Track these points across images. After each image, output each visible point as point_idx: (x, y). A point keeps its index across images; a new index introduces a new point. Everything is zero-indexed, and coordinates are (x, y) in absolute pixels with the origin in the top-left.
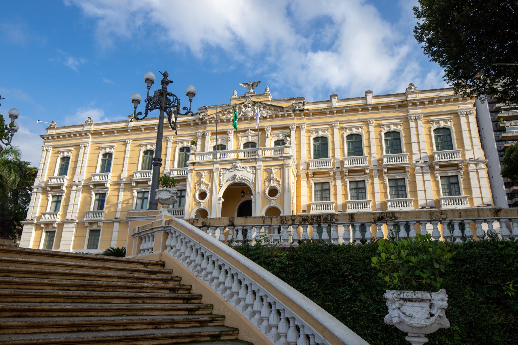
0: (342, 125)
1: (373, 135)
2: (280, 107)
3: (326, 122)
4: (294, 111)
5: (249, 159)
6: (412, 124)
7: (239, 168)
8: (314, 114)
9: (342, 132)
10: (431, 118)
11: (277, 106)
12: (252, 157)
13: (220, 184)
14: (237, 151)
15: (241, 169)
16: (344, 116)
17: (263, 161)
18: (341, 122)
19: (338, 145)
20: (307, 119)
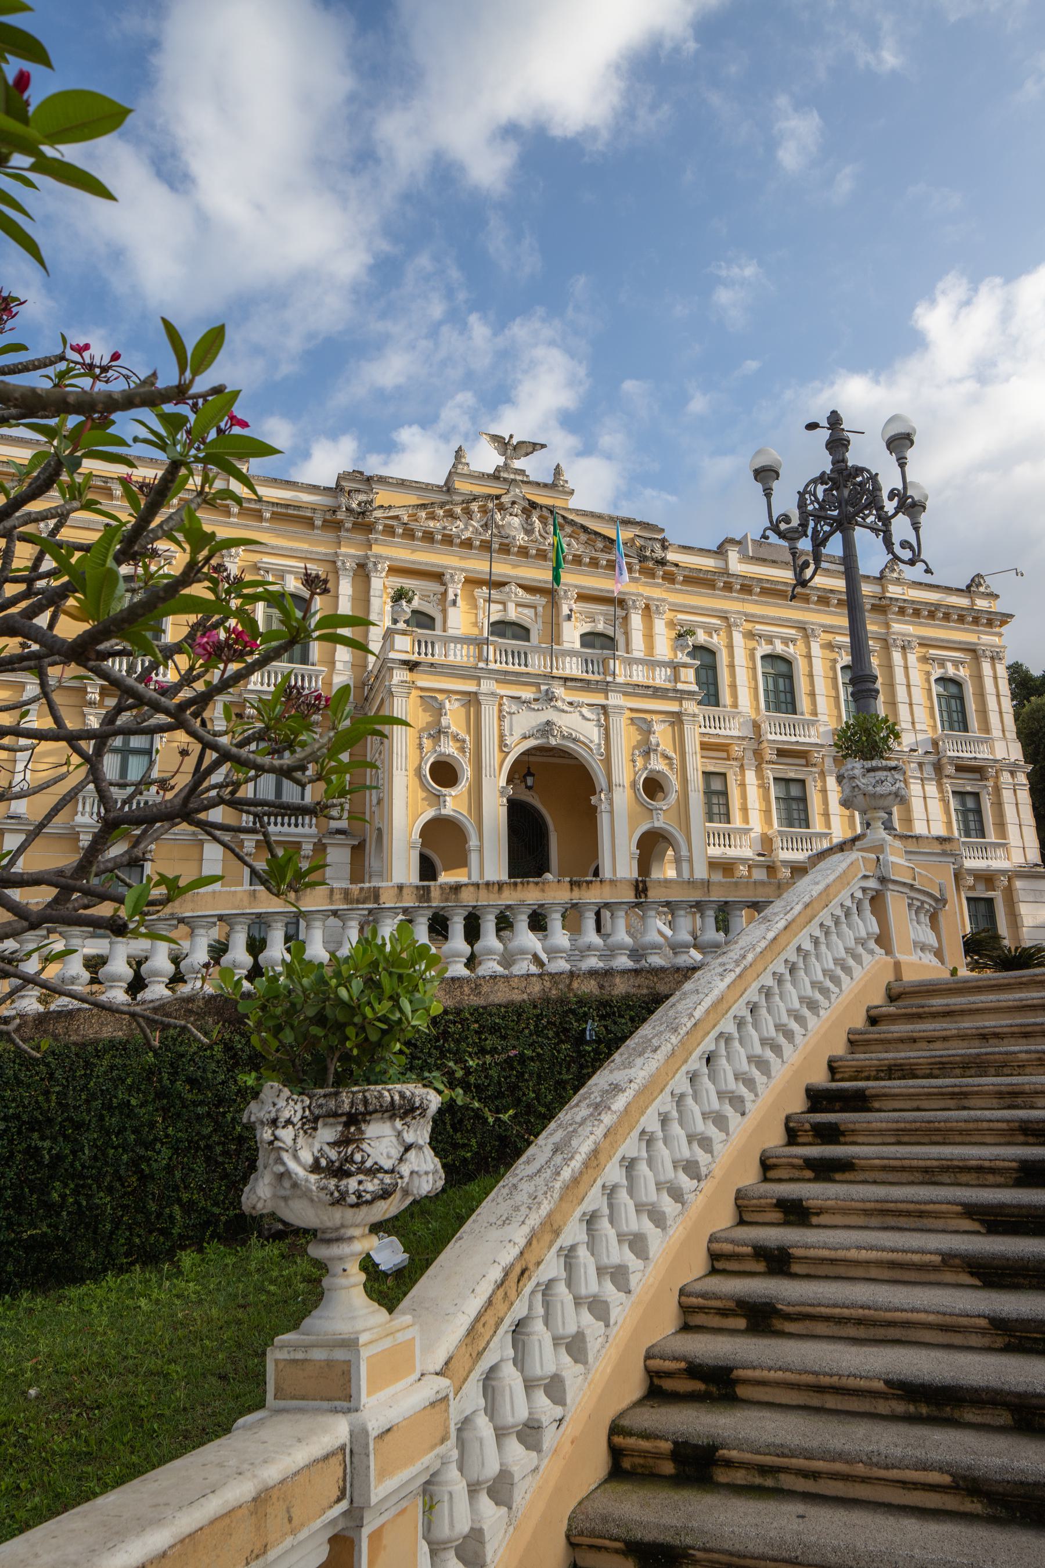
0: (749, 626)
1: (819, 667)
2: (606, 538)
3: (716, 610)
4: (643, 559)
5: (589, 682)
6: (897, 656)
7: (559, 704)
8: (689, 580)
9: (752, 644)
10: (931, 651)
11: (596, 533)
12: (597, 677)
13: (502, 744)
14: (652, 664)
15: (566, 708)
16: (756, 602)
17: (625, 694)
18: (750, 618)
19: (742, 676)
20: (668, 590)
